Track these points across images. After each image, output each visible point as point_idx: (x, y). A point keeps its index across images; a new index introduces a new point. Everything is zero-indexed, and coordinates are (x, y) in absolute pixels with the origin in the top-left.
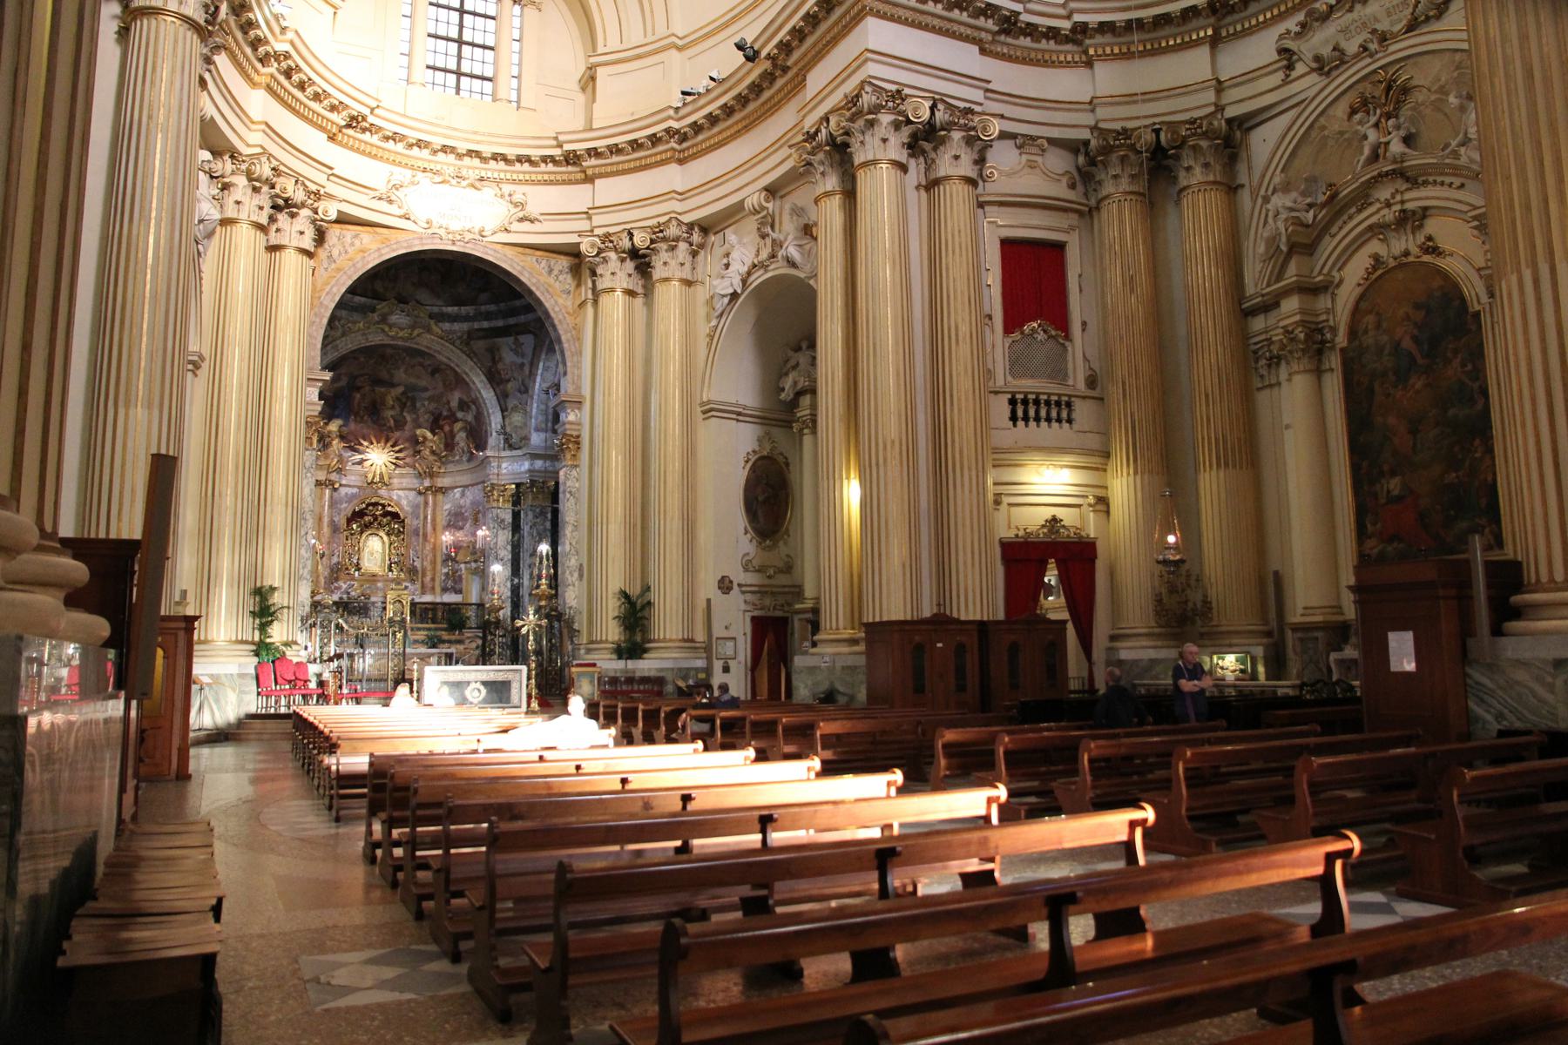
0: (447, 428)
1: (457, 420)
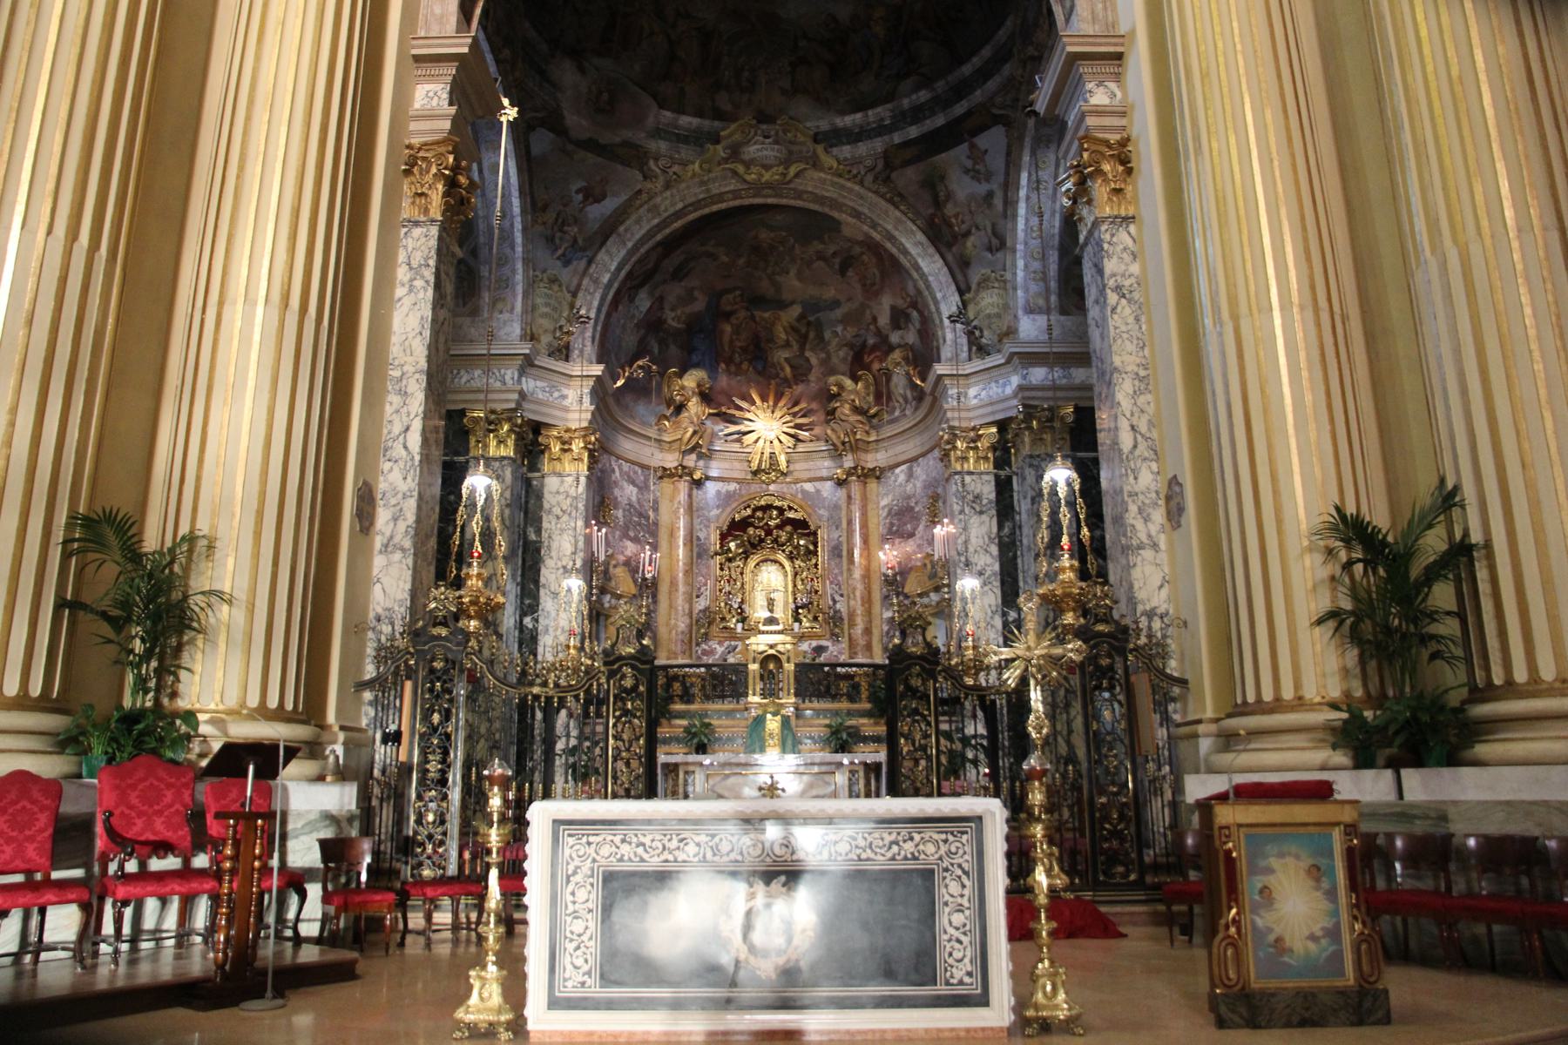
0: (876, 366)
1: (891, 349)
